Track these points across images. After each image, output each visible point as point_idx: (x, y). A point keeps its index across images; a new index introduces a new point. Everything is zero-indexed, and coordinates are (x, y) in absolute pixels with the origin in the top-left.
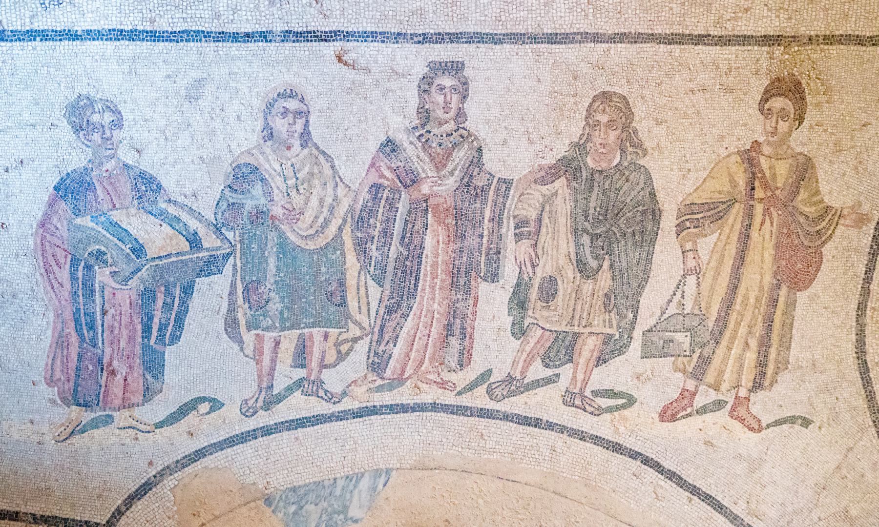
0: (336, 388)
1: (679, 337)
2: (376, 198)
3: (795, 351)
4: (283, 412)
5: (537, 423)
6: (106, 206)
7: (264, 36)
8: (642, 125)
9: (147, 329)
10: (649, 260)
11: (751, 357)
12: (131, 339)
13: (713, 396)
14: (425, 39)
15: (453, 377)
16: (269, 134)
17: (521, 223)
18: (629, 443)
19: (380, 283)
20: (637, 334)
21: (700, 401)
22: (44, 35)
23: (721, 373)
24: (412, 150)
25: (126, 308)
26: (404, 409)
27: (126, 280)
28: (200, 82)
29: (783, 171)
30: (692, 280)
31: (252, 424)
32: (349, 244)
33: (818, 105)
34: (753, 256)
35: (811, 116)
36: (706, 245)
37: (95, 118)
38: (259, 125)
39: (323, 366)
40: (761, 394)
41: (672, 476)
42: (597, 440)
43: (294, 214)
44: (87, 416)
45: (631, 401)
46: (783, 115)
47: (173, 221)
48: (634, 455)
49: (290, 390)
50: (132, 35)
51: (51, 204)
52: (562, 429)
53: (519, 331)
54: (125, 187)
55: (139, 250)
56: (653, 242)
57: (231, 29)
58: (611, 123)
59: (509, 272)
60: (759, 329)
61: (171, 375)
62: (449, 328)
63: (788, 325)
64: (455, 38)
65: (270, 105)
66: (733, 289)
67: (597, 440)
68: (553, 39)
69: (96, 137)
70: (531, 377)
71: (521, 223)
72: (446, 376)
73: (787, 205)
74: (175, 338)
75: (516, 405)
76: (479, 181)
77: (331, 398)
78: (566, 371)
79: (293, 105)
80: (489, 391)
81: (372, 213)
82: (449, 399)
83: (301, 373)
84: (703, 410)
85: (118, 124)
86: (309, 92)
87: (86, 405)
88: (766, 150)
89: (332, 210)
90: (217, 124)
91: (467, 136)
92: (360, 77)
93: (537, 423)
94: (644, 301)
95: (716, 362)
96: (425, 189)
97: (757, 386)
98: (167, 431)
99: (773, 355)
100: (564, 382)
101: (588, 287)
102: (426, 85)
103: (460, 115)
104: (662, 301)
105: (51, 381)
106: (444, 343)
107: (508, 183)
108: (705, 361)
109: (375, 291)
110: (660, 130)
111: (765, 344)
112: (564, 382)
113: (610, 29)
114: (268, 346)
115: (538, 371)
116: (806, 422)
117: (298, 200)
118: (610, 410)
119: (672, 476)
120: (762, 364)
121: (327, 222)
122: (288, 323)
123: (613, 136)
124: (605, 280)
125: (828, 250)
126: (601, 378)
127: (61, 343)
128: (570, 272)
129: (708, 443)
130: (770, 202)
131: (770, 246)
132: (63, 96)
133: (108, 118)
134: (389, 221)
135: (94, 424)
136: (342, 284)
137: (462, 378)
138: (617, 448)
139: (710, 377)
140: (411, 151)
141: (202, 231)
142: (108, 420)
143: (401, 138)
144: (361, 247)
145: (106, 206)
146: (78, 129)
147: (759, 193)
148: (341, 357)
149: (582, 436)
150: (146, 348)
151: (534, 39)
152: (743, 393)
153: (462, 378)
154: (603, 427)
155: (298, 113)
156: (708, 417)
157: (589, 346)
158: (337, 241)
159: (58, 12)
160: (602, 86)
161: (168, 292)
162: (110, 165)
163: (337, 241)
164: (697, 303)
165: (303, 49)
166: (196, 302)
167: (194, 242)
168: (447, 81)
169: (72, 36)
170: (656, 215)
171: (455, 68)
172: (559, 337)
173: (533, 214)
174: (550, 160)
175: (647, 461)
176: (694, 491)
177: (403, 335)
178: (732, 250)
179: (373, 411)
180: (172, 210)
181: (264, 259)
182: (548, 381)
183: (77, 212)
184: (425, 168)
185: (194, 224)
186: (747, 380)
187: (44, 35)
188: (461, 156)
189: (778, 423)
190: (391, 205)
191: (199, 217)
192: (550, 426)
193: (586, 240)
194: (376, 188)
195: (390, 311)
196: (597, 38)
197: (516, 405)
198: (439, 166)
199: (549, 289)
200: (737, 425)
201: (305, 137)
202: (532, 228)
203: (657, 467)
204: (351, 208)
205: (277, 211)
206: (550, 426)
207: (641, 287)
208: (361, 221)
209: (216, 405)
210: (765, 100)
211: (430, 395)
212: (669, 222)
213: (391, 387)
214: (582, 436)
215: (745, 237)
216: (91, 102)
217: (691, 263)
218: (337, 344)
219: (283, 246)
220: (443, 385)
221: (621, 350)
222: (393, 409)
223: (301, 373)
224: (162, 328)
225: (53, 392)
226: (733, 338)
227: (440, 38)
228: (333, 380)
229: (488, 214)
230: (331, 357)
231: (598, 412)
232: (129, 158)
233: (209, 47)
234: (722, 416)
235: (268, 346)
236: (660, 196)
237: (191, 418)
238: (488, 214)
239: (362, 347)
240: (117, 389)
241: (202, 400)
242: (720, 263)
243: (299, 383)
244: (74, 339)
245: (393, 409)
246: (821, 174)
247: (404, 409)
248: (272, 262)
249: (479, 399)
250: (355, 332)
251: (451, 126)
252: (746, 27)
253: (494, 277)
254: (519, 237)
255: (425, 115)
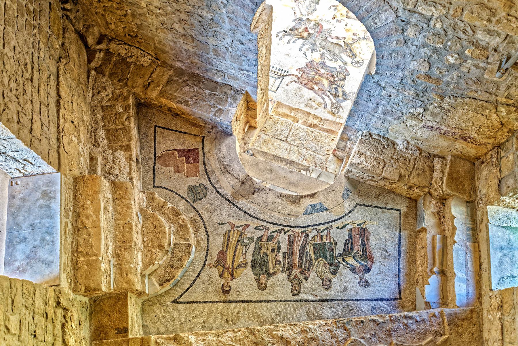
0: (314, 231)
1: (246, 241)
2: (308, 268)
3: (222, 238)
4: (325, 226)
5: (275, 224)
6: (361, 267)
7: (332, 300)
8: (256, 285)
9: (352, 243)
10: (253, 256)
11: (231, 237)
12: (354, 241)
13: (239, 229)
14: (300, 301)
15: (292, 233)
16: (330, 281)
17: (279, 264)
18: (256, 220)
19: (307, 252)
20: (255, 242)
21: (241, 228)
22: (375, 300)
23: (237, 234)
24: (302, 278)
25: (356, 247)
26: (301, 227)
27: (356, 252)
28: (344, 291)
29: (226, 274)
30: (244, 252)
31: (331, 224)
32: (313, 259)
33: (219, 289)
34: (231, 258)
35: (220, 286)
36: (241, 259)
37: (364, 284)
38: (332, 283)
39: (317, 235)
40: (229, 229)
41: (246, 213)
42: (263, 221)
43: (324, 265)
44: (362, 226)
45: (255, 228)
46: (226, 286)
47: (348, 264)
48: (254, 217)
49: (324, 231)
50: (357, 300)
51: (371, 267)
52: (269, 223)
53: (279, 242)
54: (357, 270)
55: (354, 258)
56: (252, 260)
57: (339, 302)
58: (262, 284)
59: (281, 254)
60: (230, 243)
61: (347, 233)
62: (293, 243)
63: (224, 244)
64: (294, 301)
65: (330, 287)
66: (235, 251)
67: (263, 221)
68: (275, 301)
69: (363, 280)
70: (276, 233)
71: (279, 264)
72: (293, 233)
73: (225, 268)
74: (346, 241)
75: (279, 228)
76: (288, 272)
77: (315, 229)
78: (269, 234)
79: (326, 287)
80: (284, 230)
81: (309, 265)
82: (292, 229)
83: (321, 234)
84: (241, 226)
85: (359, 283)
86: (322, 289)
87: (362, 228)
88: (229, 279)
89: (317, 266)
90: (340, 283)
91: (291, 281)
92: (313, 293)
93: (275, 224)
94: (254, 248)
95: (238, 236)
96: (299, 270)
97: (230, 231)
98: (347, 223)
99: (227, 237)
100: (269, 232)
101: (265, 251)
102: (300, 291)
103: (292, 285)
104: (250, 248)
105: (369, 233)
106: (294, 240)
107: (282, 272)
108: (241, 236)
109: (308, 250)
110: (252, 283)
111: (228, 240)
112: (269, 232)
113: (263, 303)
114: (328, 239)
115: (275, 234)
116: (219, 224)
117: (324, 268)
118: (260, 226)
119: (246, 213)
120: (229, 236)
121: (318, 263)
122: (325, 244)
123: (261, 282)
124: (262, 252)
125: (216, 259)
126: (262, 233)
127: (368, 240)
128: (269, 254)
129: (239, 219)
130: (228, 269)
131: (228, 258)
132: (370, 288)
133: (361, 284)
134: (306, 264)
135: (361, 224)
136: (314, 252)
137: (290, 233)
138: (258, 219)
139: (239, 233)
140: (302, 278)
141: (342, 262)
142: (358, 225)
143: (304, 281)
144: (311, 259)
145: (361, 267)
146: (367, 282)
147: (231, 270)
148: (314, 237)
149: (265, 221)
150: (352, 239)
151: (278, 301)
152: (232, 230)
153: (290, 233)
154: (261, 223)
155: (325, 285)
156: (239, 225)
157: (264, 239)
158: (316, 260)
159: (372, 305)
160: (264, 292)
161: (348, 250)
162: (360, 274)
163: (316, 260)
164: (243, 248)
165: (324, 298)
166: (343, 248)
167: (344, 260)
168: (295, 292)
169: (370, 300)
170: (252, 266)
171: (294, 295)
172: (271, 241)
173: (277, 265)
174: (274, 277)
175: (252, 216)
176: (242, 210)
177: (302, 242)
178: (236, 259)
179: (307, 226)
180: (348, 266)
181: (330, 256)
182: (273, 232)
183: (366, 265)
184: (299, 275)
185: (344, 263)
186: (232, 233)
187: (375, 300)
188: (292, 277)
189: (225, 224)
190: (305, 267)
191: (343, 264)
192: (272, 223)
193: (266, 261)
194: (308, 270)
195: (305, 246)
196: (265, 301)
197: (279, 228)
198: (296, 275)
199: (273, 250)
200: (234, 223)
201: (323, 280)
202: (277, 263)
203: (250, 215)
204: (313, 266)
205: (328, 266)
206: (272, 223)
207: (254, 251)
208: (311, 264)
209: (338, 228)
210: (230, 290)
211: (296, 230)
212: (249, 264)
213: (304, 231)
214: (265, 221)
215: (233, 261)
216: (365, 287)
217: (244, 256)
218: (315, 240)
219: (326, 258)
220: (294, 232)
221: (258, 239)
222: (303, 227)
223: (322, 234)
224: (349, 243)
225: (369, 230)
226: (235, 241)
227: (297, 301)
228: (315, 233)
229: (286, 266)
230: (316, 237)
231: (262, 226)
232: (357, 276)
233: (343, 298)
234: (237, 225)
235: (328, 239)
236: (251, 269)
237: (342, 225)
238: (286, 266)
239: (310, 239)
240: (357, 231)
241: (340, 229)
242: (238, 256)
243: (322, 232)
244: (365, 241)
245: (303, 227)
246: (218, 274)
247: (301, 227)
248: (328, 256)
249: (286, 229)
250: (311, 242)
251: (294, 283)
252: (235, 304)
253: (285, 253)
254: (280, 261)
255: (299, 285)
